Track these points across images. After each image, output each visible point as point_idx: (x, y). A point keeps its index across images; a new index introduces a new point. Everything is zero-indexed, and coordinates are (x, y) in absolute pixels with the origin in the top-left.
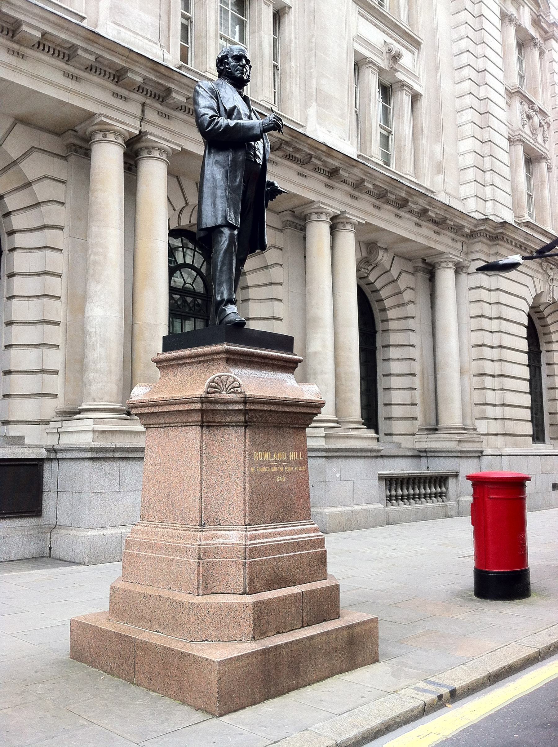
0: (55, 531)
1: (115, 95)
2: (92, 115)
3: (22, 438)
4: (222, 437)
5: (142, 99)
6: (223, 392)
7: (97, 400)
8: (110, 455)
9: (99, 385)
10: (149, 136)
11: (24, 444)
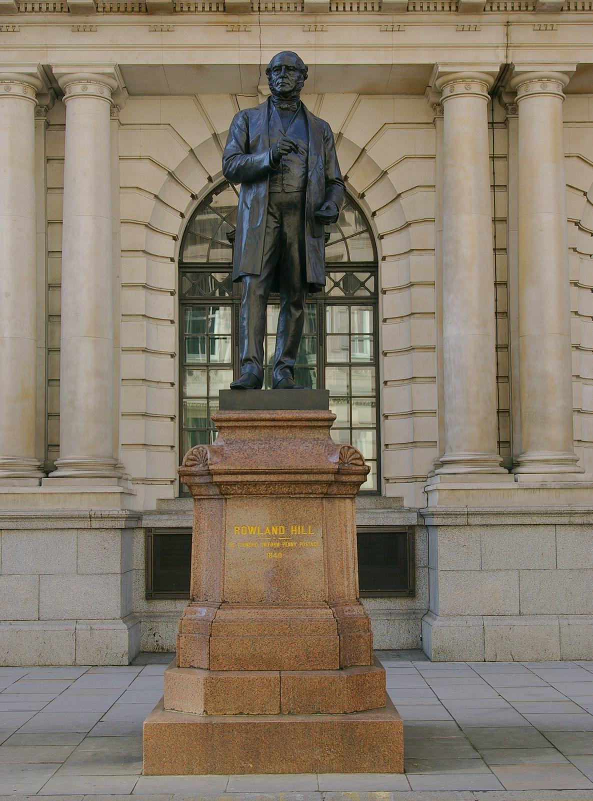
0: (426, 618)
2: (431, 68)
3: (400, 499)
4: (211, 511)
5: (501, 17)
6: (201, 465)
10: (517, 69)
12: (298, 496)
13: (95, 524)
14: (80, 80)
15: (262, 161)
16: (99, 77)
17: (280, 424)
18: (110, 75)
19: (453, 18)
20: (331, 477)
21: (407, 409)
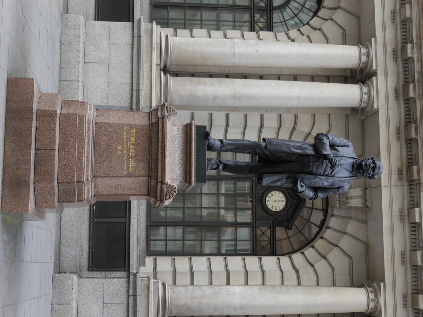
1: (405, 296)
3: (144, 264)
7: (172, 290)
8: (131, 293)
9: (183, 291)
11: (140, 266)
12: (150, 163)
13: (135, 93)
14: (370, 91)
15: (326, 150)
16: (371, 101)
17: (188, 156)
18: (372, 106)
19: (410, 292)
20: (160, 180)
21: (194, 269)
